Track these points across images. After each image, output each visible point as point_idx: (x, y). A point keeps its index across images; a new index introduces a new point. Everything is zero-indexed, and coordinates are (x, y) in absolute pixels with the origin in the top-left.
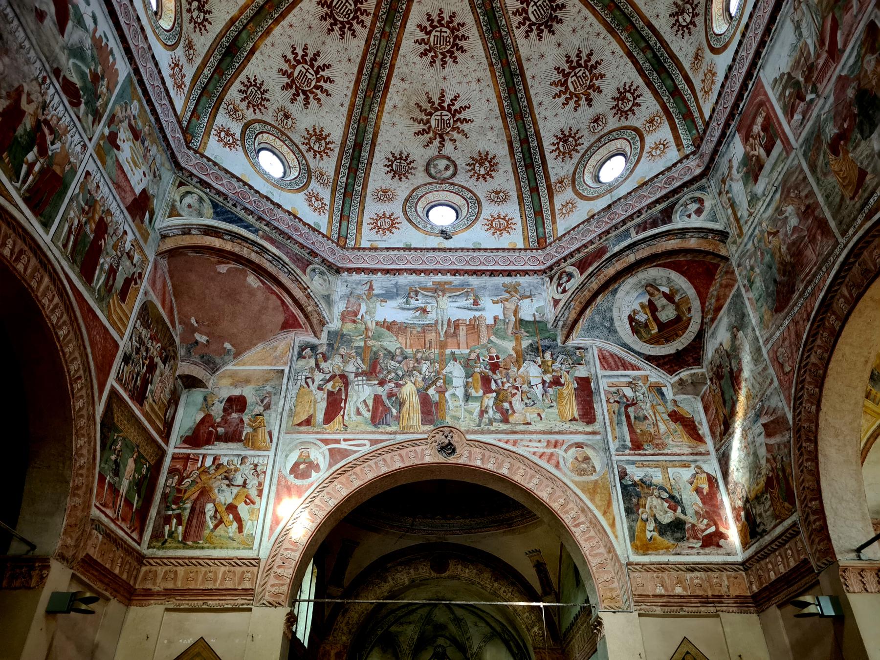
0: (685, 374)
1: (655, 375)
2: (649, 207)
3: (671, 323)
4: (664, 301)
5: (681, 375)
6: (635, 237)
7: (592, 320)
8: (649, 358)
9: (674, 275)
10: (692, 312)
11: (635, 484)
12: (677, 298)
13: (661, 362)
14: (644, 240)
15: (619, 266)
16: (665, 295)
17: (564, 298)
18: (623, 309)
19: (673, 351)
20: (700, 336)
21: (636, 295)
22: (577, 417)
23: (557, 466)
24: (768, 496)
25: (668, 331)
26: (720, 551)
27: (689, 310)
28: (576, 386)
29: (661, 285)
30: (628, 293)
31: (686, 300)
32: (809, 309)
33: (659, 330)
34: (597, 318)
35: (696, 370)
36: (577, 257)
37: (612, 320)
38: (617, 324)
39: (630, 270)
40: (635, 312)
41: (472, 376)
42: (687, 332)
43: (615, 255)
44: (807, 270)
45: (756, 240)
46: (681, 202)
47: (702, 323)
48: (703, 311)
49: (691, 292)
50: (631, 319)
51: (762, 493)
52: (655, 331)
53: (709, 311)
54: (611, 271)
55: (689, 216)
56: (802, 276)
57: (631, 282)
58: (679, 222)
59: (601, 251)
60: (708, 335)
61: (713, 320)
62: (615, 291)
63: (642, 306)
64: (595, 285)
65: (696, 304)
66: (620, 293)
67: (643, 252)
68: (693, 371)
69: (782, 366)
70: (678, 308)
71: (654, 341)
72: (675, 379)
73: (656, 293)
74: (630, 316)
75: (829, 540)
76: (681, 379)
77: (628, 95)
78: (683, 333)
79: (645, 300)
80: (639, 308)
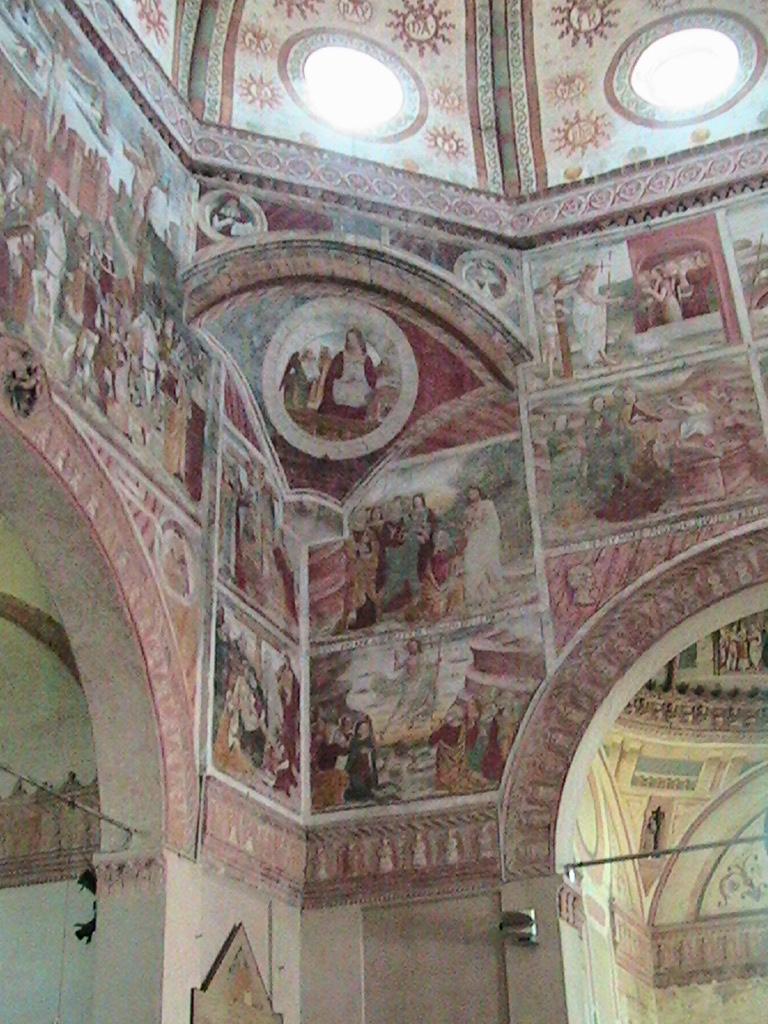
0: (311, 498)
1: (275, 476)
2: (426, 220)
3: (345, 411)
4: (360, 372)
5: (305, 498)
6: (383, 244)
7: (241, 318)
8: (278, 441)
9: (404, 347)
10: (389, 417)
11: (228, 644)
12: (381, 382)
13: (291, 458)
14: (398, 263)
15: (340, 269)
16: (368, 362)
17: (222, 245)
18: (294, 336)
19: (318, 454)
20: (374, 458)
21: (328, 330)
22: (183, 474)
23: (151, 549)
24: (434, 751)
25: (333, 418)
26: (289, 804)
27: (387, 410)
28: (190, 417)
29: (374, 346)
30: (318, 318)
31: (394, 394)
32: (676, 547)
33: (320, 410)
34: (250, 321)
35: (330, 503)
36: (280, 197)
37: (268, 341)
38: (271, 352)
39: (351, 285)
40: (307, 354)
41: (74, 270)
42: (359, 440)
43: (341, 246)
44: (700, 498)
45: (599, 404)
46: (474, 254)
47: (390, 444)
48: (404, 428)
49: (410, 388)
50: (294, 361)
51: (418, 744)
52: (314, 404)
53: (414, 433)
54: (322, 265)
55: (481, 286)
56: (684, 500)
57: (335, 305)
58: (461, 279)
59: (317, 222)
60: (390, 463)
61: (414, 451)
62: (303, 300)
63: (324, 354)
64: (284, 264)
65: (403, 410)
66: (307, 310)
67: (389, 280)
68: (324, 502)
69: (573, 591)
70: (371, 397)
71: (301, 418)
72: (292, 497)
73: (359, 351)
74: (296, 355)
75: (552, 843)
76: (301, 503)
77: (431, 20)
78: (351, 438)
79: (335, 348)
80: (317, 353)
